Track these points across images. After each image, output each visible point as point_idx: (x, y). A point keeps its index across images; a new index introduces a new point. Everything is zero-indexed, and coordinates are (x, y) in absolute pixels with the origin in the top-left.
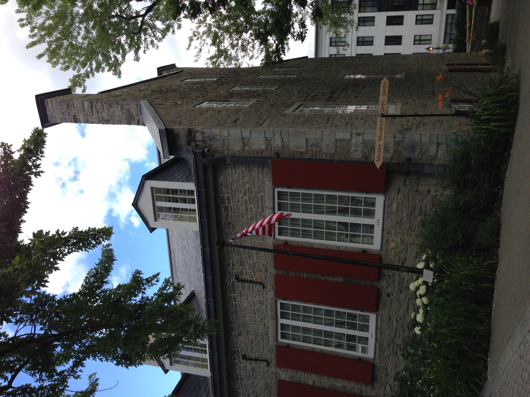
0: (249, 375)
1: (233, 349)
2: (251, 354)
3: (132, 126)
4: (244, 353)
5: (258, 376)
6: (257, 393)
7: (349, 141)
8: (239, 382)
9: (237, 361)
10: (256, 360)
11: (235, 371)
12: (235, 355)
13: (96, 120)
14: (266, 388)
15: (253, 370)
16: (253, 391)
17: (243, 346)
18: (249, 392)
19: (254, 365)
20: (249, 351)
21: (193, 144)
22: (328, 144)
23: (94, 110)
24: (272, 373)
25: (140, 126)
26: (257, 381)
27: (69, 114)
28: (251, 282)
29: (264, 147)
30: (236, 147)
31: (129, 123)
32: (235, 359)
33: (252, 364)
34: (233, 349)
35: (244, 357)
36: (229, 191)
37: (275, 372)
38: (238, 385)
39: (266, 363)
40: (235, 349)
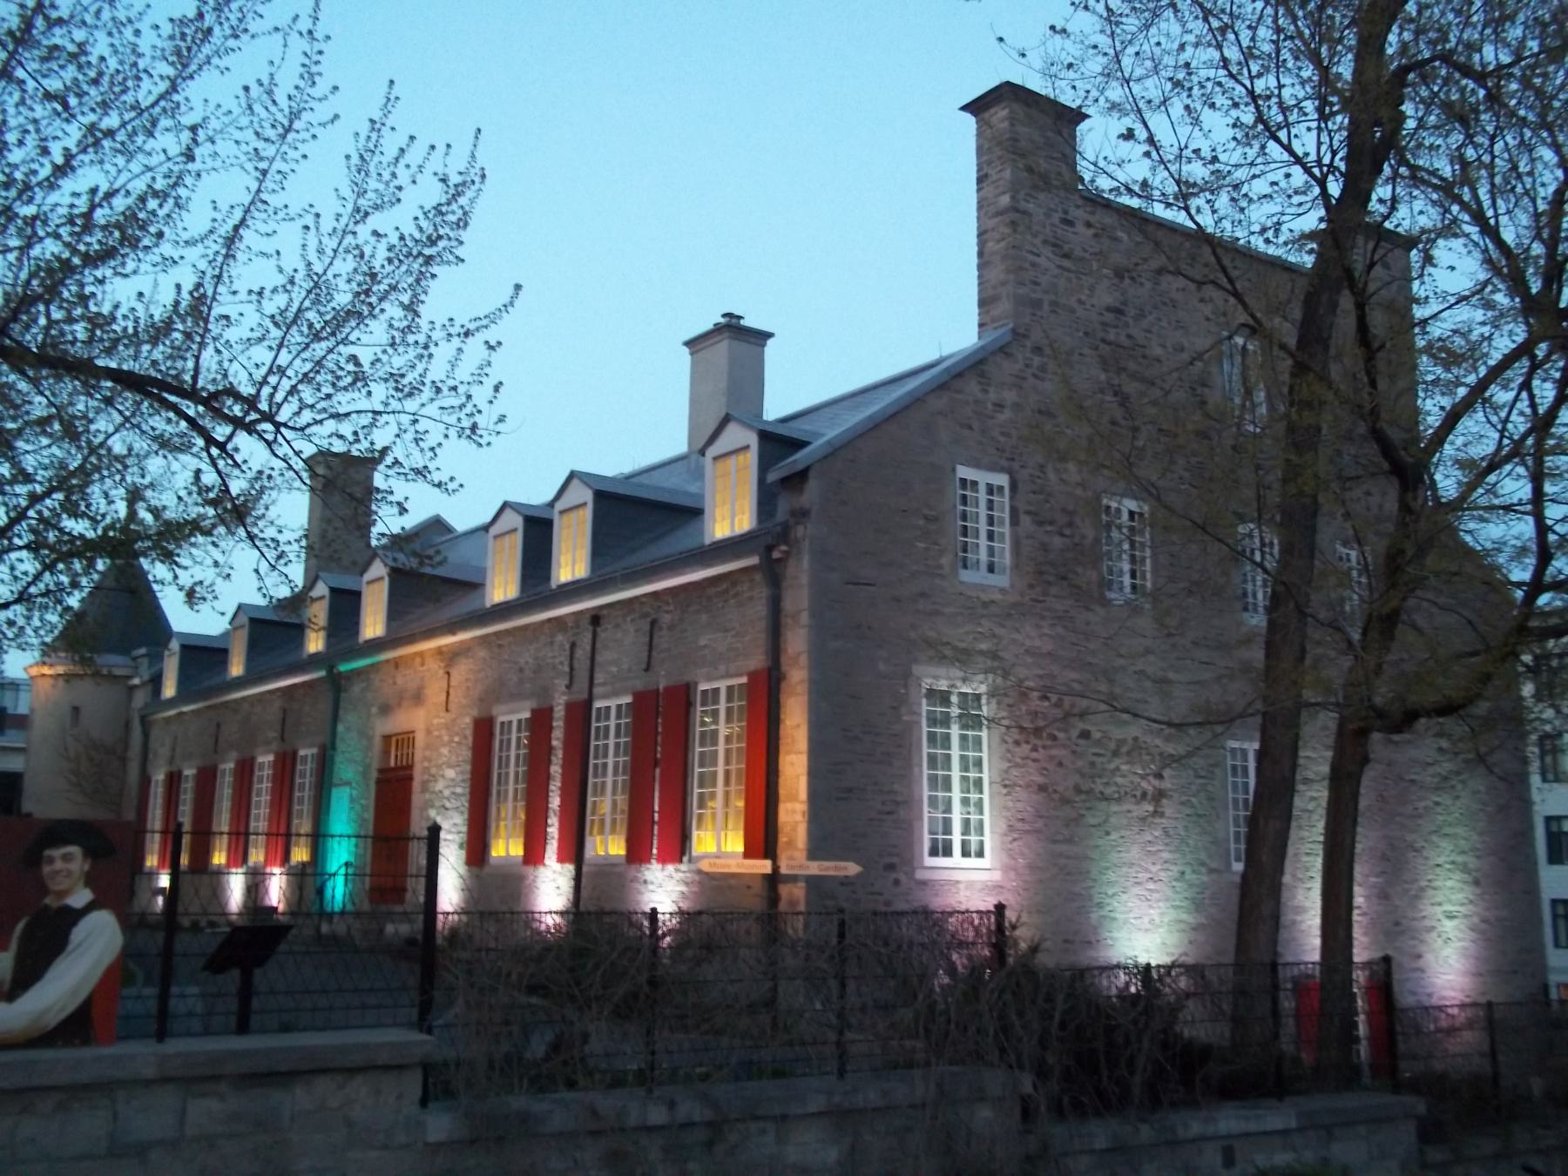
13: (983, 228)
22: (792, 764)
23: (996, 220)
25: (976, 329)
27: (989, 163)
30: (788, 605)
31: (983, 303)
35: (573, 646)
36: (745, 595)
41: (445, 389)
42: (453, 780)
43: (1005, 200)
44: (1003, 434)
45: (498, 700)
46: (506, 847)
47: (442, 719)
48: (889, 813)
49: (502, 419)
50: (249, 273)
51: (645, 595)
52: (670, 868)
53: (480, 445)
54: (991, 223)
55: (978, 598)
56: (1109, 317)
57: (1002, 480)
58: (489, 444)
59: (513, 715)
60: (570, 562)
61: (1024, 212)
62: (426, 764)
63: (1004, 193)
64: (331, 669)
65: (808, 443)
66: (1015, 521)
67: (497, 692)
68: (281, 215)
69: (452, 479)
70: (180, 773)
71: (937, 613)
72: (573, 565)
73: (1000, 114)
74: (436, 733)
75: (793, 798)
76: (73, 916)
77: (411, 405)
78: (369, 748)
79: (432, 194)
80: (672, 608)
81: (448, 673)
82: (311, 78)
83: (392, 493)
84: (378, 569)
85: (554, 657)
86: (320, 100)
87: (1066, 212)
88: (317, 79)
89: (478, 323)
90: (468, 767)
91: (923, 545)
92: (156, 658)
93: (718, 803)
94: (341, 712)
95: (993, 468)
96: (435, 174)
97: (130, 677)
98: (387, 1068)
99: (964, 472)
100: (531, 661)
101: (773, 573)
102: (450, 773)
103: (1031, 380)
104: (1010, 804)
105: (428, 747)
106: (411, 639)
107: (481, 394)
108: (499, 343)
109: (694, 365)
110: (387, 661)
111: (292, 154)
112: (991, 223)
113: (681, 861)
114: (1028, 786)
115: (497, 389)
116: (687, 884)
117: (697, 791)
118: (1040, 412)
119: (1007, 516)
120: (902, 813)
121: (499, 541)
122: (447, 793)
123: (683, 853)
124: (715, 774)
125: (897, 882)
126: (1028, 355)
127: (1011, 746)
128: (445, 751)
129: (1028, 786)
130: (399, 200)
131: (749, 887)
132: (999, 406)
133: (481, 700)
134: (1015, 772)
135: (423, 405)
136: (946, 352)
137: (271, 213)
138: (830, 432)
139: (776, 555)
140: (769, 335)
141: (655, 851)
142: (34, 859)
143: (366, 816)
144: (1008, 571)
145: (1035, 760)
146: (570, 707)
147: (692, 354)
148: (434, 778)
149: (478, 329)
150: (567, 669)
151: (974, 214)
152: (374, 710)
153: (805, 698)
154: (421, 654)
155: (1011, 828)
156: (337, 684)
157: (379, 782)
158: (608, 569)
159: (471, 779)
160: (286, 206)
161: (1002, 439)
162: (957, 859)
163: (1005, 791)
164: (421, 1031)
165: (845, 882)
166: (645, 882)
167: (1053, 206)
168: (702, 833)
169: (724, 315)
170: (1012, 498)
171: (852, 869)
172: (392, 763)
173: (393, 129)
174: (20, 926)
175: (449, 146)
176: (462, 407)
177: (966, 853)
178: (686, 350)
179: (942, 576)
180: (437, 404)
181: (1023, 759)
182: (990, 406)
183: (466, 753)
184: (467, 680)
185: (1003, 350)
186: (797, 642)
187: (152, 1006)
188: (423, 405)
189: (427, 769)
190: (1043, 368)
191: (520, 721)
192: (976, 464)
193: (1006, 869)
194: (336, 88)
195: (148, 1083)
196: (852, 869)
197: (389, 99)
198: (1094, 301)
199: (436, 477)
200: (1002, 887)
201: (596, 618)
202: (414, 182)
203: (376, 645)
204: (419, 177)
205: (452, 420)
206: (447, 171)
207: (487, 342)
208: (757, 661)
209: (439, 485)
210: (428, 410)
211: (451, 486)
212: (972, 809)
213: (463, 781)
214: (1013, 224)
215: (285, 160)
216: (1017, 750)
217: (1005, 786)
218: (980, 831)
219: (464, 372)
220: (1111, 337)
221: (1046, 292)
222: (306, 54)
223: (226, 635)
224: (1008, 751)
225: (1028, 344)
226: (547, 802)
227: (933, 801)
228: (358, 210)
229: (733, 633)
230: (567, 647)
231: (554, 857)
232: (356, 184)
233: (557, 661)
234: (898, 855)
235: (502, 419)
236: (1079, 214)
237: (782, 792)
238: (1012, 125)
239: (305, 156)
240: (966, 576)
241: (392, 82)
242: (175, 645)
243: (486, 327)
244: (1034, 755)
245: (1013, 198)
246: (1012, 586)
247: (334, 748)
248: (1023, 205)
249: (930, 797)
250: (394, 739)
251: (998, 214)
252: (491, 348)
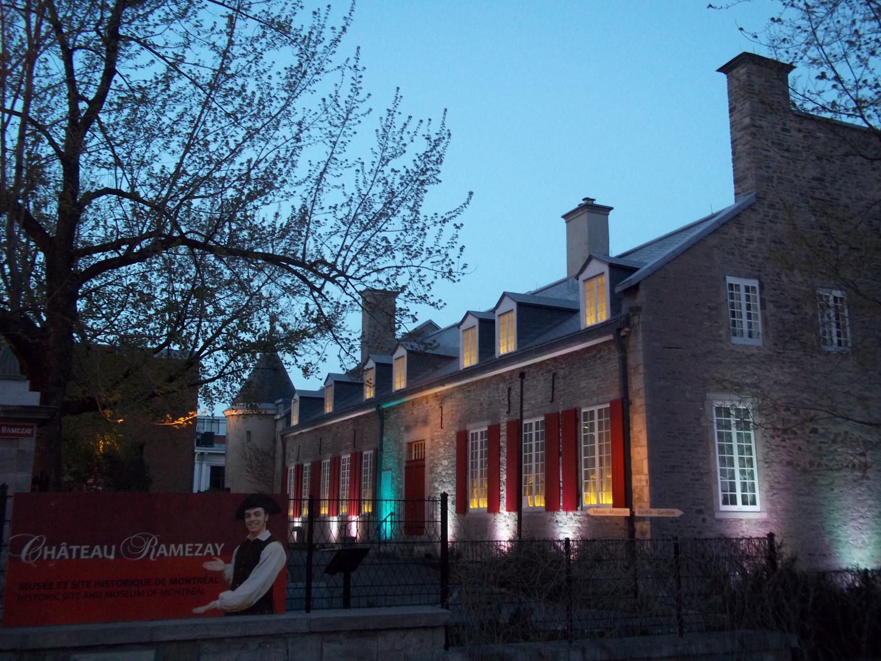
3: (733, 186)
7: (642, 473)
13: (734, 138)
21: (631, 314)
22: (639, 453)
23: (742, 132)
25: (733, 197)
28: (553, 388)
29: (634, 388)
30: (631, 362)
31: (736, 181)
36: (606, 357)
41: (434, 252)
42: (447, 466)
43: (747, 121)
44: (753, 256)
45: (469, 421)
46: (478, 503)
47: (439, 432)
48: (697, 480)
49: (465, 266)
50: (330, 197)
51: (548, 360)
52: (571, 513)
53: (454, 281)
54: (738, 135)
55: (743, 353)
56: (815, 183)
57: (754, 283)
58: (459, 280)
59: (479, 429)
60: (505, 343)
61: (761, 127)
62: (432, 458)
63: (746, 117)
64: (378, 406)
65: (637, 269)
66: (763, 306)
67: (468, 417)
68: (344, 165)
69: (440, 301)
70: (302, 465)
71: (720, 362)
72: (508, 344)
73: (742, 71)
74: (436, 440)
75: (640, 472)
76: (261, 545)
77: (416, 262)
78: (401, 450)
79: (422, 146)
80: (564, 366)
81: (441, 407)
82: (356, 90)
83: (408, 310)
84: (401, 352)
85: (499, 396)
86: (361, 102)
87: (784, 124)
88: (360, 91)
89: (451, 215)
90: (455, 459)
91: (708, 324)
92: (287, 404)
93: (597, 476)
94: (384, 430)
95: (748, 276)
96: (424, 135)
97: (274, 415)
98: (425, 628)
99: (730, 280)
100: (486, 399)
101: (622, 344)
102: (445, 462)
103: (768, 223)
104: (771, 473)
105: (432, 448)
106: (421, 389)
107: (453, 253)
108: (462, 225)
109: (568, 228)
110: (408, 402)
111: (349, 132)
112: (738, 135)
113: (577, 510)
114: (781, 462)
115: (462, 249)
116: (581, 522)
117: (583, 469)
118: (775, 242)
119: (758, 304)
120: (705, 480)
121: (465, 333)
122: (443, 473)
123: (578, 505)
124: (594, 459)
125: (704, 520)
126: (766, 209)
127: (769, 439)
128: (442, 450)
129: (781, 462)
130: (404, 151)
131: (617, 524)
132: (750, 240)
133: (460, 421)
134: (772, 454)
135: (423, 261)
136: (715, 211)
137: (339, 164)
138: (650, 261)
139: (623, 334)
140: (611, 209)
141: (561, 504)
142: (241, 516)
143: (401, 487)
144: (761, 336)
145: (784, 447)
146: (509, 424)
147: (567, 223)
148: (436, 466)
149: (450, 218)
150: (507, 403)
151: (729, 130)
152: (402, 429)
153: (644, 415)
154: (426, 397)
155: (772, 487)
156: (382, 416)
157: (406, 468)
158: (528, 346)
159: (457, 465)
160: (347, 160)
161: (753, 259)
162: (739, 506)
163: (766, 466)
164: (442, 607)
165: (674, 520)
166: (557, 521)
167: (776, 121)
168: (588, 493)
169: (584, 200)
170: (760, 293)
171: (678, 513)
172: (413, 458)
173: (400, 113)
174: (236, 550)
175: (430, 120)
176: (443, 261)
177: (745, 503)
178: (563, 221)
179: (721, 341)
180: (430, 260)
181: (776, 446)
182: (744, 241)
183: (453, 451)
184: (452, 411)
185: (750, 208)
186: (637, 383)
187: (303, 592)
188: (423, 261)
189: (433, 460)
190: (775, 216)
191: (482, 433)
192: (738, 275)
193: (770, 512)
194: (369, 95)
195: (304, 634)
196: (678, 513)
197: (397, 98)
198: (805, 175)
199: (432, 300)
200: (768, 522)
201: (522, 374)
202: (412, 141)
203: (402, 393)
204: (415, 138)
205: (438, 268)
206: (430, 133)
207: (455, 225)
208: (615, 394)
209: (433, 305)
210: (427, 264)
211: (440, 305)
212: (747, 476)
213: (452, 466)
214: (753, 134)
215: (345, 136)
216: (773, 441)
217: (767, 463)
218: (753, 489)
219: (443, 243)
220: (817, 195)
221: (775, 172)
222: (353, 78)
223: (322, 390)
224: (767, 442)
225: (765, 202)
226: (500, 478)
227: (723, 473)
228: (383, 158)
229: (600, 379)
230: (506, 390)
231: (505, 508)
232: (382, 145)
233: (501, 398)
234: (704, 504)
235: (465, 266)
236: (792, 124)
237: (633, 469)
238: (749, 77)
239: (355, 133)
240: (736, 340)
241: (398, 88)
242: (296, 397)
243: (455, 216)
244: (783, 444)
245: (752, 119)
246: (764, 345)
247: (382, 450)
248: (758, 123)
249: (721, 470)
250: (414, 444)
251: (744, 129)
252: (458, 227)
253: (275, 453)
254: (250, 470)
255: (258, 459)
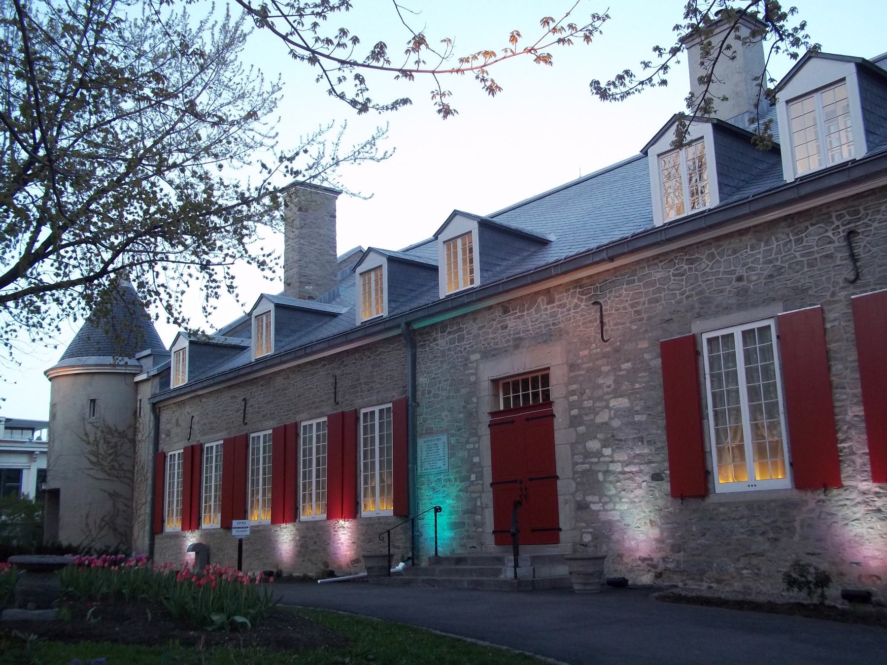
0: (813, 252)
1: (861, 208)
2: (862, 244)
4: (860, 231)
5: (815, 268)
6: (779, 275)
8: (792, 238)
9: (837, 223)
10: (854, 258)
11: (812, 225)
12: (849, 214)
14: (795, 289)
15: (826, 256)
16: (782, 267)
17: (876, 224)
18: (777, 259)
19: (840, 255)
20: (868, 238)
24: (833, 294)
26: (806, 269)
32: (840, 217)
33: (840, 251)
34: (861, 208)
35: (851, 234)
37: (836, 298)
38: (783, 237)
39: (852, 277)
40: (862, 212)
45: (699, 316)
97: (135, 375)
172: (502, 408)
253: (135, 430)
254: (94, 459)
255: (109, 443)
